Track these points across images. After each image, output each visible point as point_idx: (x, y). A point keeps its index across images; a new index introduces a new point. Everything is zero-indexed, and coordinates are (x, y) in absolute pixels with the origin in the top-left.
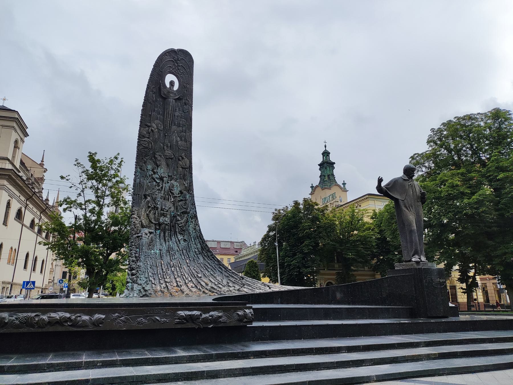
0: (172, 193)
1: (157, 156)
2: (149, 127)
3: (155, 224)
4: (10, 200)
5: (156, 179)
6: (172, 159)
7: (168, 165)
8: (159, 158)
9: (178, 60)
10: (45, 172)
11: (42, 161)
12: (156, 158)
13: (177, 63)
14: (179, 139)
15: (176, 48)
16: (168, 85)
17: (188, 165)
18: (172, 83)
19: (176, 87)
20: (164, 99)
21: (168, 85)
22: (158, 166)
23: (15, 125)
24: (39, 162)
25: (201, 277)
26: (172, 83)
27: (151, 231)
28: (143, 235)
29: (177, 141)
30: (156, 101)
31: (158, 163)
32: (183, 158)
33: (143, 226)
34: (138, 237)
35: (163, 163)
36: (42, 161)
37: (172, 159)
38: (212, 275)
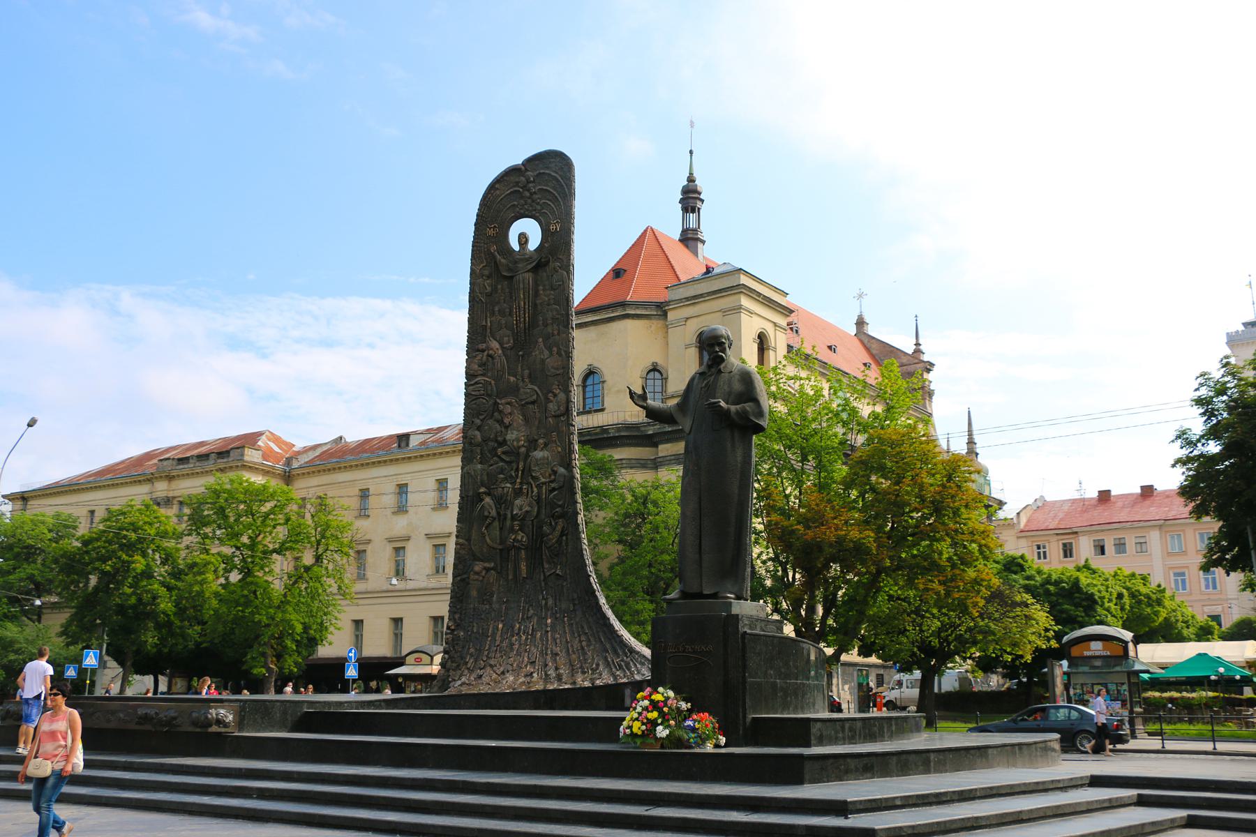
0: (533, 478)
2: (483, 351)
5: (503, 457)
6: (533, 403)
7: (527, 420)
9: (528, 182)
10: (928, 371)
11: (918, 344)
12: (500, 412)
13: (528, 190)
14: (546, 352)
15: (519, 161)
16: (516, 247)
18: (523, 239)
19: (534, 244)
20: (512, 277)
21: (515, 246)
22: (507, 427)
23: (745, 302)
24: (910, 351)
25: (557, 654)
26: (523, 239)
27: (487, 565)
29: (543, 361)
30: (495, 290)
31: (506, 421)
32: (555, 395)
33: (476, 558)
35: (519, 419)
36: (918, 344)
37: (533, 403)
38: (582, 648)
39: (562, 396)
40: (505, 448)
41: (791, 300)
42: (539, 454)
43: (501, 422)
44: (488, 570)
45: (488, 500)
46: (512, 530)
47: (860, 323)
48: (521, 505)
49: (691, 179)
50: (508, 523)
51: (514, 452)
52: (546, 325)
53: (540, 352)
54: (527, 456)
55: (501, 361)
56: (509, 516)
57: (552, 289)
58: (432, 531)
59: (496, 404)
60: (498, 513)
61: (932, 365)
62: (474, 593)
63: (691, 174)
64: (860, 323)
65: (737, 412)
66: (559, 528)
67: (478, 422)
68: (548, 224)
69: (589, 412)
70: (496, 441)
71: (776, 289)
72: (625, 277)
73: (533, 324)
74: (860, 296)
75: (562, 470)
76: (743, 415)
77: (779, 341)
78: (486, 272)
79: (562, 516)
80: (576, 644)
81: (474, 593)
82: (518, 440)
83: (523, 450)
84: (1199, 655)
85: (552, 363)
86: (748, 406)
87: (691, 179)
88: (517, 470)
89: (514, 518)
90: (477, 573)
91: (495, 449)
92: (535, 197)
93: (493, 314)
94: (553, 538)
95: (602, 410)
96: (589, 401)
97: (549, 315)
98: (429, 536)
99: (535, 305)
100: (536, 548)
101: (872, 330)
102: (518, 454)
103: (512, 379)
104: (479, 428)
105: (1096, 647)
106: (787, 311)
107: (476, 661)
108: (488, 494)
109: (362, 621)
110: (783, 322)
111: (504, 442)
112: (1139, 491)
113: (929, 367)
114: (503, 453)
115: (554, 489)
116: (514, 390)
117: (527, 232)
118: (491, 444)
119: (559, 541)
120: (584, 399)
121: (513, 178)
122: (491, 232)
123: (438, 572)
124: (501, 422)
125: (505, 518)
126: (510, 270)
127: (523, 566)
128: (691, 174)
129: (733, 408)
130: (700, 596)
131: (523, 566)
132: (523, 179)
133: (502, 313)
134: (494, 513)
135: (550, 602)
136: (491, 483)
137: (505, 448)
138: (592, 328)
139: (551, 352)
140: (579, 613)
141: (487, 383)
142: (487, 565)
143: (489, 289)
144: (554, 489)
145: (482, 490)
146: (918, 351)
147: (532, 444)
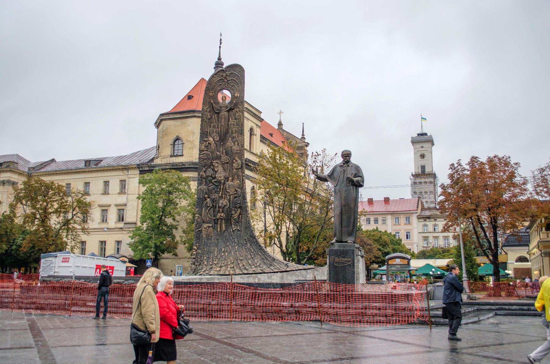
1: (214, 164)
2: (206, 141)
3: (214, 220)
4: (253, 187)
7: (224, 170)
8: (216, 165)
10: (307, 146)
11: (303, 135)
12: (213, 166)
14: (233, 144)
17: (240, 166)
19: (228, 101)
20: (219, 113)
22: (216, 172)
24: (300, 138)
28: (203, 229)
29: (231, 147)
31: (216, 169)
32: (236, 161)
33: (204, 222)
34: (199, 231)
36: (303, 135)
37: (227, 163)
39: (239, 161)
40: (215, 180)
41: (262, 116)
42: (230, 183)
43: (213, 170)
44: (209, 227)
45: (209, 199)
46: (219, 212)
47: (280, 124)
48: (223, 202)
49: (219, 59)
50: (217, 208)
51: (220, 182)
52: (232, 133)
53: (230, 143)
54: (224, 183)
55: (213, 146)
56: (217, 206)
57: (235, 119)
58: (101, 203)
59: (211, 162)
60: (213, 205)
61: (308, 144)
62: (204, 236)
63: (219, 56)
64: (280, 124)
65: (356, 181)
66: (239, 212)
67: (204, 169)
68: (235, 93)
69: (176, 156)
70: (212, 177)
71: (258, 110)
72: (193, 99)
73: (227, 132)
74: (281, 113)
75: (239, 190)
76: (358, 182)
77: (258, 132)
78: (208, 110)
79: (240, 207)
80: (249, 256)
81: (204, 236)
82: (220, 177)
83: (222, 181)
84: (427, 264)
85: (235, 148)
86: (359, 178)
87: (219, 59)
88: (220, 189)
89: (219, 207)
90: (205, 228)
91: (211, 180)
92: (229, 82)
93: (210, 127)
94: (236, 216)
95: (182, 155)
96: (175, 151)
97: (234, 129)
98: (100, 206)
99: (228, 125)
100: (228, 220)
101: (284, 128)
102: (221, 182)
103: (218, 153)
104: (205, 172)
105: (398, 261)
106: (261, 120)
107: (208, 262)
108: (209, 197)
109: (85, 242)
110: (259, 123)
111: (215, 178)
112: (383, 199)
113: (307, 145)
114: (215, 182)
115: (236, 197)
116: (219, 158)
117: (226, 95)
118: (210, 178)
119: (239, 217)
120: (174, 150)
121: (221, 74)
122: (211, 94)
123: (103, 221)
124: (213, 170)
125: (216, 207)
126: (218, 110)
127: (224, 226)
128: (219, 56)
129: (355, 179)
130: (342, 242)
131: (224, 226)
132: (225, 74)
133: (214, 127)
134: (211, 205)
135: (236, 240)
136: (209, 192)
137: (215, 180)
138: (179, 120)
139: (234, 143)
140: (249, 245)
141: (207, 154)
142: (208, 225)
143: (209, 117)
144: (236, 197)
145: (206, 196)
146: (303, 138)
147: (227, 179)
